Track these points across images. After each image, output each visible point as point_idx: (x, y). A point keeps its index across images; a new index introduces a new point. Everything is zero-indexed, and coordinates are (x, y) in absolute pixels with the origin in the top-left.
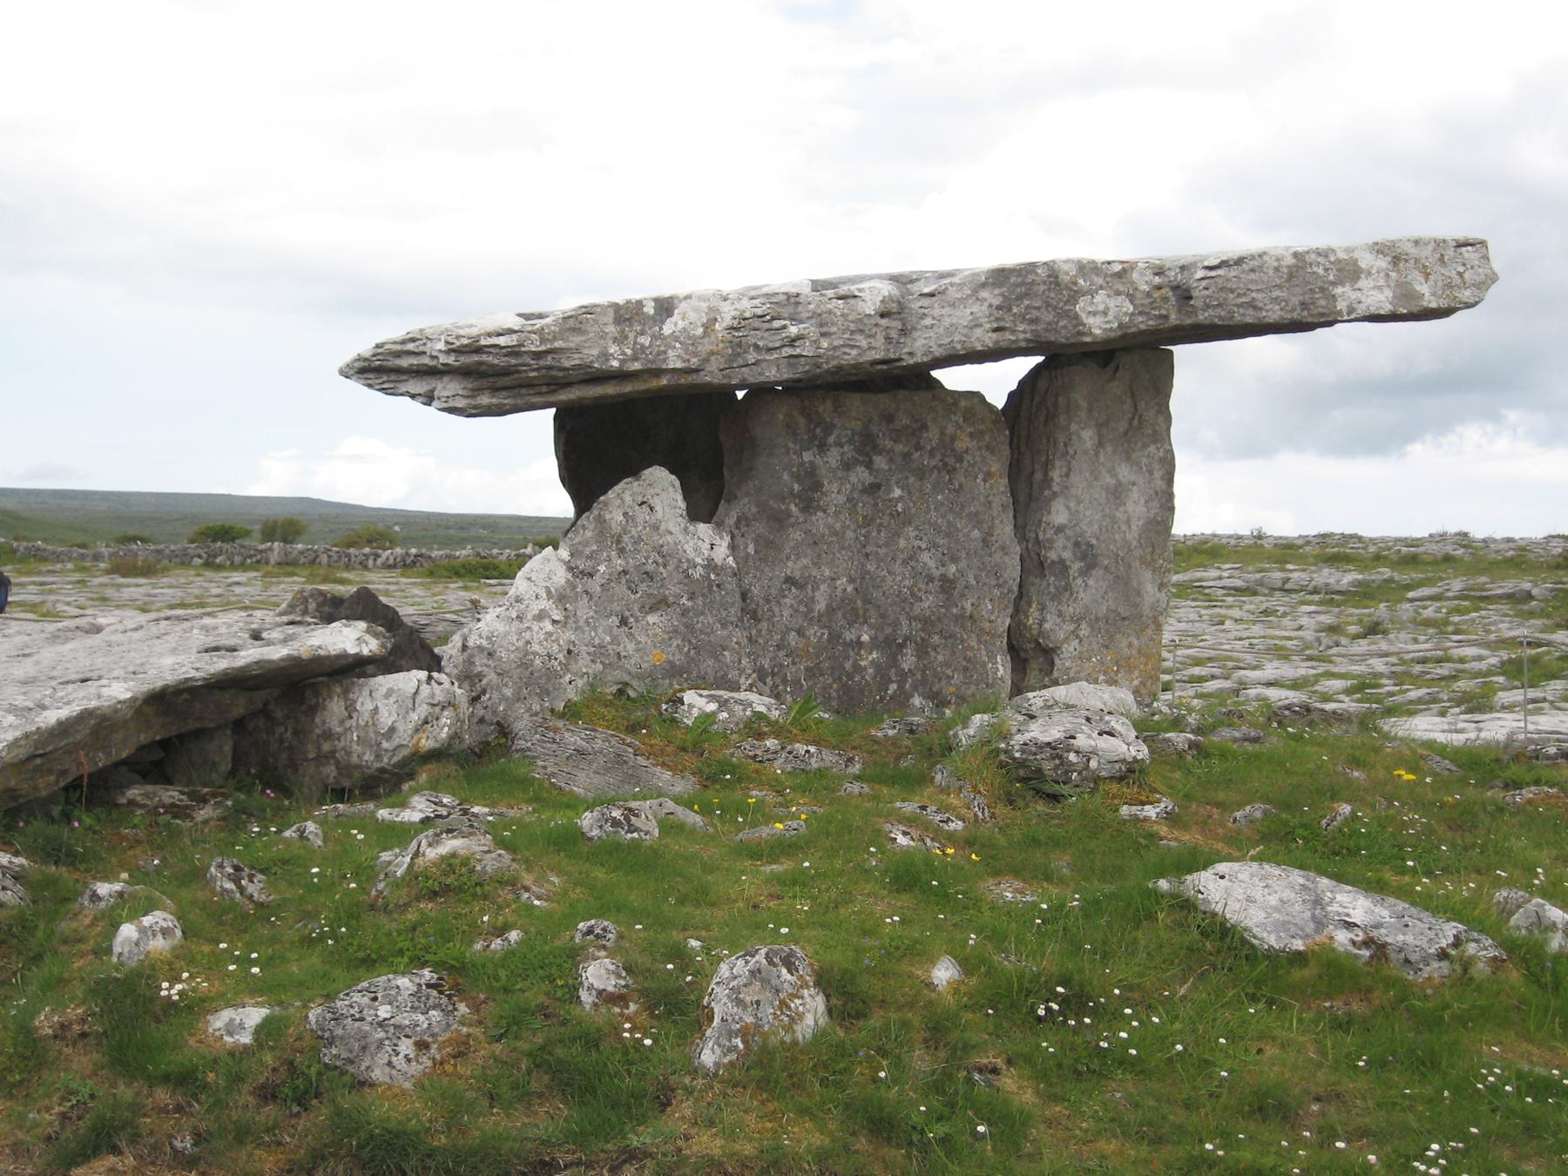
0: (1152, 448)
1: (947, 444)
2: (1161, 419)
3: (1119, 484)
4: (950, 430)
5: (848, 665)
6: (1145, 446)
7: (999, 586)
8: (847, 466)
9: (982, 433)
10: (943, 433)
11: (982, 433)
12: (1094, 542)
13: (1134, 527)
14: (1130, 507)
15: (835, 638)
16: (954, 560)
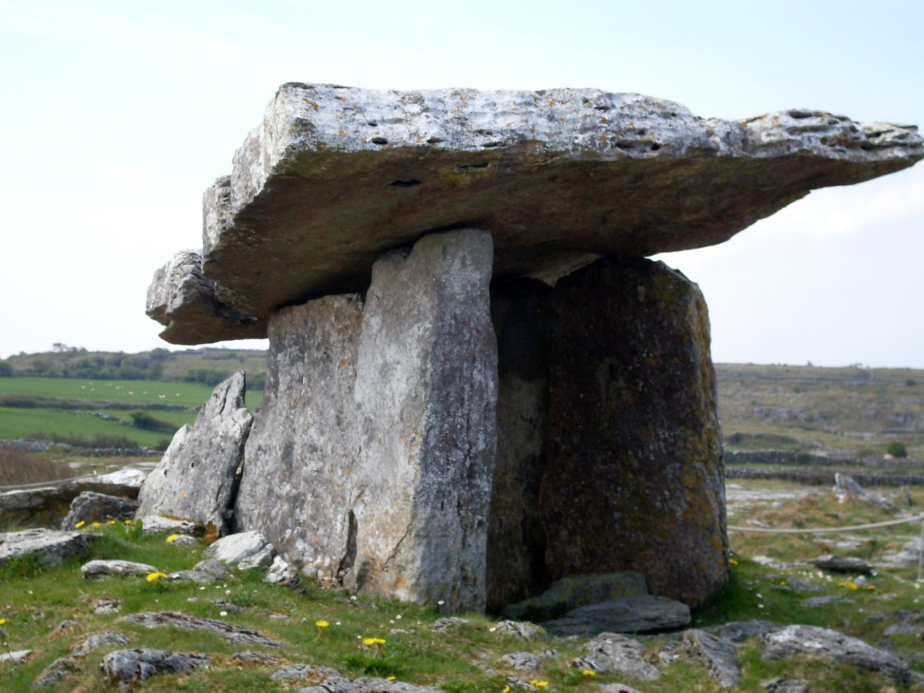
0: (415, 329)
1: (325, 343)
2: (425, 299)
3: (387, 364)
4: (327, 328)
5: (273, 513)
6: (411, 326)
7: (346, 456)
8: (292, 363)
9: (346, 327)
10: (324, 332)
11: (346, 327)
12: (372, 417)
13: (397, 403)
14: (394, 384)
15: (270, 492)
16: (322, 433)
